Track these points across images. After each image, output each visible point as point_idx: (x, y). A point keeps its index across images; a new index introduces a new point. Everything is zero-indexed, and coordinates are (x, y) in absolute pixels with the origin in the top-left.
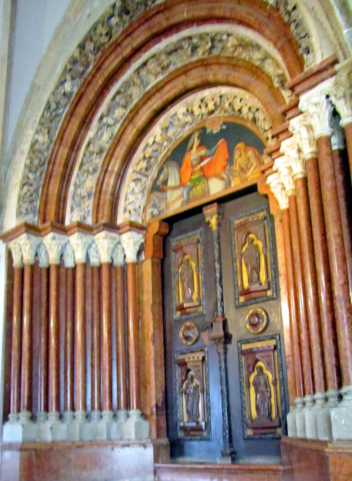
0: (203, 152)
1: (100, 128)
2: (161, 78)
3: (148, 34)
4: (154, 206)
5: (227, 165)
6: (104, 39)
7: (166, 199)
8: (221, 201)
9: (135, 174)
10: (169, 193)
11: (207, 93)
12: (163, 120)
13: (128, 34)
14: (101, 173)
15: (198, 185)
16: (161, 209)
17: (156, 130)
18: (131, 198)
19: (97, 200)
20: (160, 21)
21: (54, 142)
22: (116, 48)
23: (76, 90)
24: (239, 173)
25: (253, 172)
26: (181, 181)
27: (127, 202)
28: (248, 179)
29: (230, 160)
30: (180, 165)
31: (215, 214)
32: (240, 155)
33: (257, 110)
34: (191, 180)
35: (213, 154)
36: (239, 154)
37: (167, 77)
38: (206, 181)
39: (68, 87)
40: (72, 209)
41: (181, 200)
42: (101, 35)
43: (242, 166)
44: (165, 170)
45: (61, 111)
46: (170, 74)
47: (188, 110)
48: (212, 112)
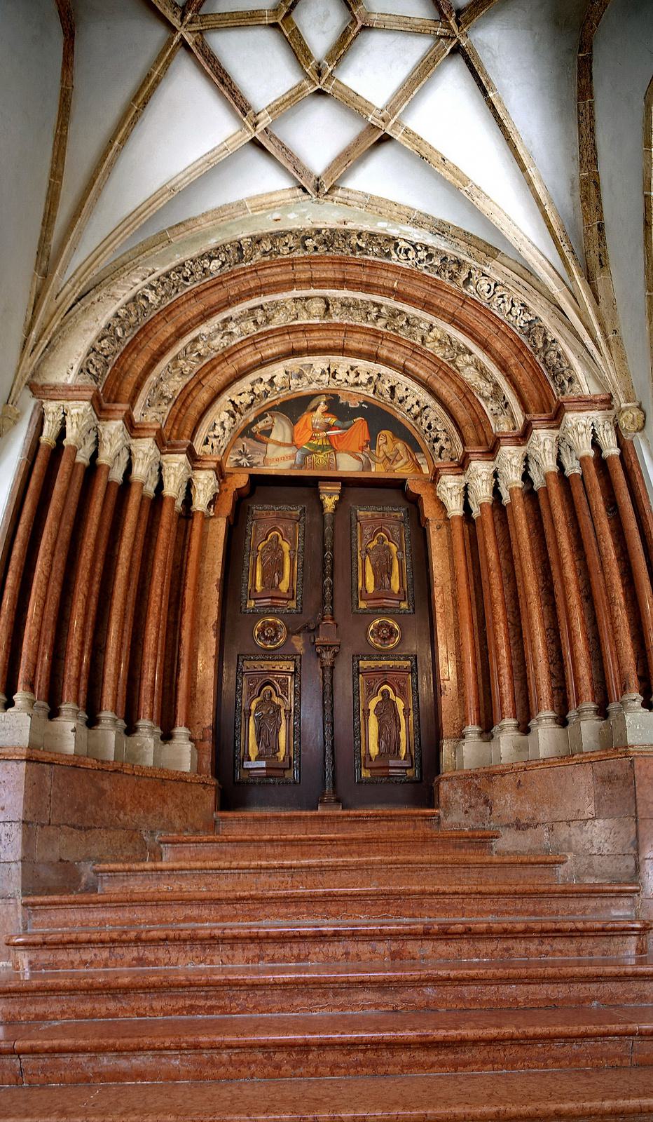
0: (333, 420)
1: (218, 330)
2: (317, 321)
8: (348, 483)
10: (270, 446)
11: (361, 363)
12: (292, 363)
13: (310, 262)
15: (319, 454)
16: (255, 461)
17: (278, 371)
20: (354, 273)
26: (293, 440)
27: (212, 434)
29: (372, 443)
30: (294, 421)
31: (336, 494)
32: (386, 443)
34: (310, 445)
35: (347, 428)
40: (145, 408)
41: (293, 461)
42: (287, 244)
43: (388, 455)
44: (269, 418)
47: (329, 369)
48: (357, 384)
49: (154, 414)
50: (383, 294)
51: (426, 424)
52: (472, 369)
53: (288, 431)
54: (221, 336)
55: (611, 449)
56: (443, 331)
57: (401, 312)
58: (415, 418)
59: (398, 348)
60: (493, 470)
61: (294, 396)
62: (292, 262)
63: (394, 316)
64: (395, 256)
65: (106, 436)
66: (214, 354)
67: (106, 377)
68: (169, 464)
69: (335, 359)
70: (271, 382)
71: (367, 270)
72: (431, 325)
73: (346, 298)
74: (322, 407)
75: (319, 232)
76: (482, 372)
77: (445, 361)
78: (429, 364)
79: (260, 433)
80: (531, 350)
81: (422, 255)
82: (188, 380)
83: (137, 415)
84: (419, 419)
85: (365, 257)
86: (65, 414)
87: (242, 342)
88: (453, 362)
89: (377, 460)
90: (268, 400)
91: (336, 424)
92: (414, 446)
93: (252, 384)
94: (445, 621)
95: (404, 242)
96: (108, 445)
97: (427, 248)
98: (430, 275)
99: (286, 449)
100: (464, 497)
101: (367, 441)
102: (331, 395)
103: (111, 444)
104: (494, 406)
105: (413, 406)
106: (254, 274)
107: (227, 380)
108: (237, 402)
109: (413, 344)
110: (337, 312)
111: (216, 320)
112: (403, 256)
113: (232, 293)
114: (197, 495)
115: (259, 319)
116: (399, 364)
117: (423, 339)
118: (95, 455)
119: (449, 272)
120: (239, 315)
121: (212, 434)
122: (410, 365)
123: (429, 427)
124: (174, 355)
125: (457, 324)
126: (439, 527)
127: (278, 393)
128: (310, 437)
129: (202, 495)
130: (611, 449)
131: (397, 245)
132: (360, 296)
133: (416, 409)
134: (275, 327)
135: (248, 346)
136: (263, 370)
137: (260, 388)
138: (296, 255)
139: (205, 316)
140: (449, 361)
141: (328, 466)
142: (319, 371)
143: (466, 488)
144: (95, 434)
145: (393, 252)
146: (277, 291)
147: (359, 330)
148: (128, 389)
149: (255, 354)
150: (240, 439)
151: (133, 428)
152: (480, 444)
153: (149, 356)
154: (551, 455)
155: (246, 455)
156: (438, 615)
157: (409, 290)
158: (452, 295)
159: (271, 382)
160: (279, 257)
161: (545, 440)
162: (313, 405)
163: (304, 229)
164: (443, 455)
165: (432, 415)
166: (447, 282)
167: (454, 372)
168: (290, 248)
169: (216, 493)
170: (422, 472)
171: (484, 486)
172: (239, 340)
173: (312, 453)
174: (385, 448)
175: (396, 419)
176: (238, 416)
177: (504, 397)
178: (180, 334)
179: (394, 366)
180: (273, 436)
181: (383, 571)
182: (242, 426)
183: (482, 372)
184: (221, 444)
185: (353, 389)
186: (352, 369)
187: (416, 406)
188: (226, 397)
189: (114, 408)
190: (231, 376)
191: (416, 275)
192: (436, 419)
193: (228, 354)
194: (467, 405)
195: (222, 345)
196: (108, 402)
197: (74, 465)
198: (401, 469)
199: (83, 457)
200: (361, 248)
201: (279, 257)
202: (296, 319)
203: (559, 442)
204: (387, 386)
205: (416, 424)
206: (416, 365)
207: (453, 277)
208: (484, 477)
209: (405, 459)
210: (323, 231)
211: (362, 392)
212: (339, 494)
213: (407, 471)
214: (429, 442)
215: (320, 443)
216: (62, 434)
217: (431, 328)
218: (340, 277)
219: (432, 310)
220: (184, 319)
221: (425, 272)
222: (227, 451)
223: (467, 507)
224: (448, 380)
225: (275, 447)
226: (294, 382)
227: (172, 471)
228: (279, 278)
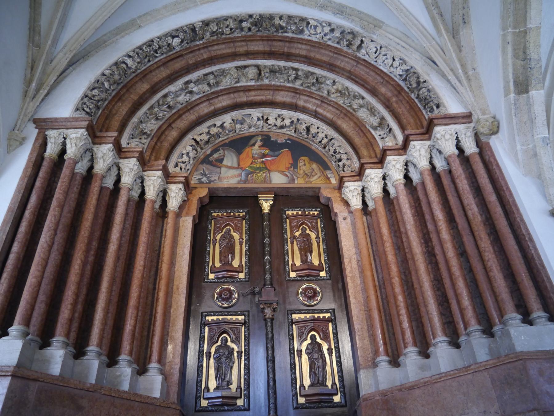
0: (267, 151)
1: (182, 90)
2: (252, 83)
3: (267, 49)
4: (204, 175)
5: (291, 167)
6: (227, 31)
10: (223, 170)
12: (236, 114)
13: (246, 40)
14: (163, 124)
15: (258, 173)
16: (212, 179)
17: (227, 119)
18: (185, 158)
19: (153, 143)
20: (278, 46)
21: (136, 73)
22: (230, 42)
23: (178, 49)
24: (303, 177)
25: (317, 179)
26: (239, 164)
28: (312, 183)
29: (295, 165)
34: (250, 167)
35: (277, 156)
36: (303, 163)
37: (258, 86)
38: (267, 172)
39: (176, 41)
40: (129, 139)
41: (239, 179)
43: (306, 172)
44: (221, 151)
45: (157, 55)
46: (261, 85)
47: (263, 117)
48: (282, 127)
49: (137, 143)
50: (299, 62)
51: (332, 150)
52: (364, 110)
53: (235, 159)
54: (184, 94)
55: (470, 148)
56: (343, 85)
57: (313, 73)
58: (324, 148)
60: (382, 174)
61: (239, 137)
62: (233, 41)
63: (307, 77)
64: (307, 32)
65: (100, 155)
66: (180, 106)
67: (98, 116)
68: (149, 178)
70: (222, 126)
71: (287, 44)
72: (334, 81)
73: (273, 65)
75: (251, 16)
76: (372, 111)
77: (345, 106)
78: (334, 110)
79: (215, 161)
80: (407, 90)
81: (327, 29)
82: (161, 123)
83: (124, 142)
84: (327, 148)
85: (286, 34)
86: (65, 138)
87: (200, 98)
88: (350, 106)
89: (298, 175)
90: (220, 139)
91: (268, 154)
92: (325, 166)
93: (209, 127)
94: (354, 282)
95: (313, 21)
96: (101, 161)
97: (330, 25)
98: (333, 45)
99: (234, 170)
100: (362, 197)
101: (291, 164)
102: (265, 135)
103: (104, 160)
105: (323, 139)
106: (206, 50)
108: (198, 140)
109: (322, 96)
110: (267, 75)
111: (180, 83)
112: (312, 32)
113: (191, 62)
114: (171, 200)
115: (212, 82)
116: (312, 111)
117: (328, 92)
118: (91, 168)
119: (346, 41)
120: (196, 78)
121: (180, 160)
122: (320, 110)
123: (335, 152)
124: (150, 106)
125: (352, 79)
126: (345, 219)
127: (227, 135)
128: (250, 162)
129: (174, 200)
130: (470, 148)
131: (308, 23)
132: (282, 63)
133: (325, 141)
134: (224, 88)
135: (205, 101)
136: (216, 119)
137: (214, 130)
138: (236, 35)
139: (171, 79)
140: (348, 106)
141: (264, 181)
142: (256, 118)
143: (363, 190)
144: (91, 154)
145: (305, 29)
146: (223, 62)
147: (283, 88)
148: (116, 123)
149: (210, 106)
150: (201, 165)
151: (120, 151)
152: (371, 157)
153: (131, 104)
154: (425, 158)
155: (206, 175)
156: (348, 278)
157: (318, 56)
158: (349, 58)
159: (222, 126)
160: (224, 36)
161: (421, 148)
162: (252, 142)
163: (241, 15)
165: (336, 144)
166: (345, 49)
167: (351, 113)
168: (231, 29)
169: (185, 201)
170: (330, 183)
171: (376, 186)
172: (198, 97)
173: (253, 173)
174: (304, 167)
175: (311, 149)
176: (199, 149)
178: (153, 91)
179: (308, 113)
180: (225, 162)
181: (306, 249)
182: (202, 157)
183: (372, 111)
184: (188, 167)
185: (280, 131)
186: (279, 116)
187: (325, 139)
188: (190, 136)
189: (105, 135)
191: (323, 46)
192: (340, 146)
193: (190, 107)
194: (362, 134)
195: (185, 100)
196: (101, 131)
197: (73, 174)
198: (316, 181)
199: (81, 168)
200: (282, 28)
201: (224, 36)
202: (237, 82)
203: (431, 149)
204: (304, 126)
205: (326, 152)
206: (324, 110)
207: (349, 45)
208: (376, 179)
209: (319, 175)
210: (254, 16)
212: (273, 200)
213: (320, 182)
214: (335, 162)
215: (258, 166)
216: (63, 151)
217: (334, 82)
218: (268, 49)
219: (334, 71)
220: (156, 80)
221: (329, 43)
222: (192, 173)
223: (364, 203)
224: (347, 119)
225: (226, 169)
226: (238, 126)
227: (151, 182)
228: (224, 51)
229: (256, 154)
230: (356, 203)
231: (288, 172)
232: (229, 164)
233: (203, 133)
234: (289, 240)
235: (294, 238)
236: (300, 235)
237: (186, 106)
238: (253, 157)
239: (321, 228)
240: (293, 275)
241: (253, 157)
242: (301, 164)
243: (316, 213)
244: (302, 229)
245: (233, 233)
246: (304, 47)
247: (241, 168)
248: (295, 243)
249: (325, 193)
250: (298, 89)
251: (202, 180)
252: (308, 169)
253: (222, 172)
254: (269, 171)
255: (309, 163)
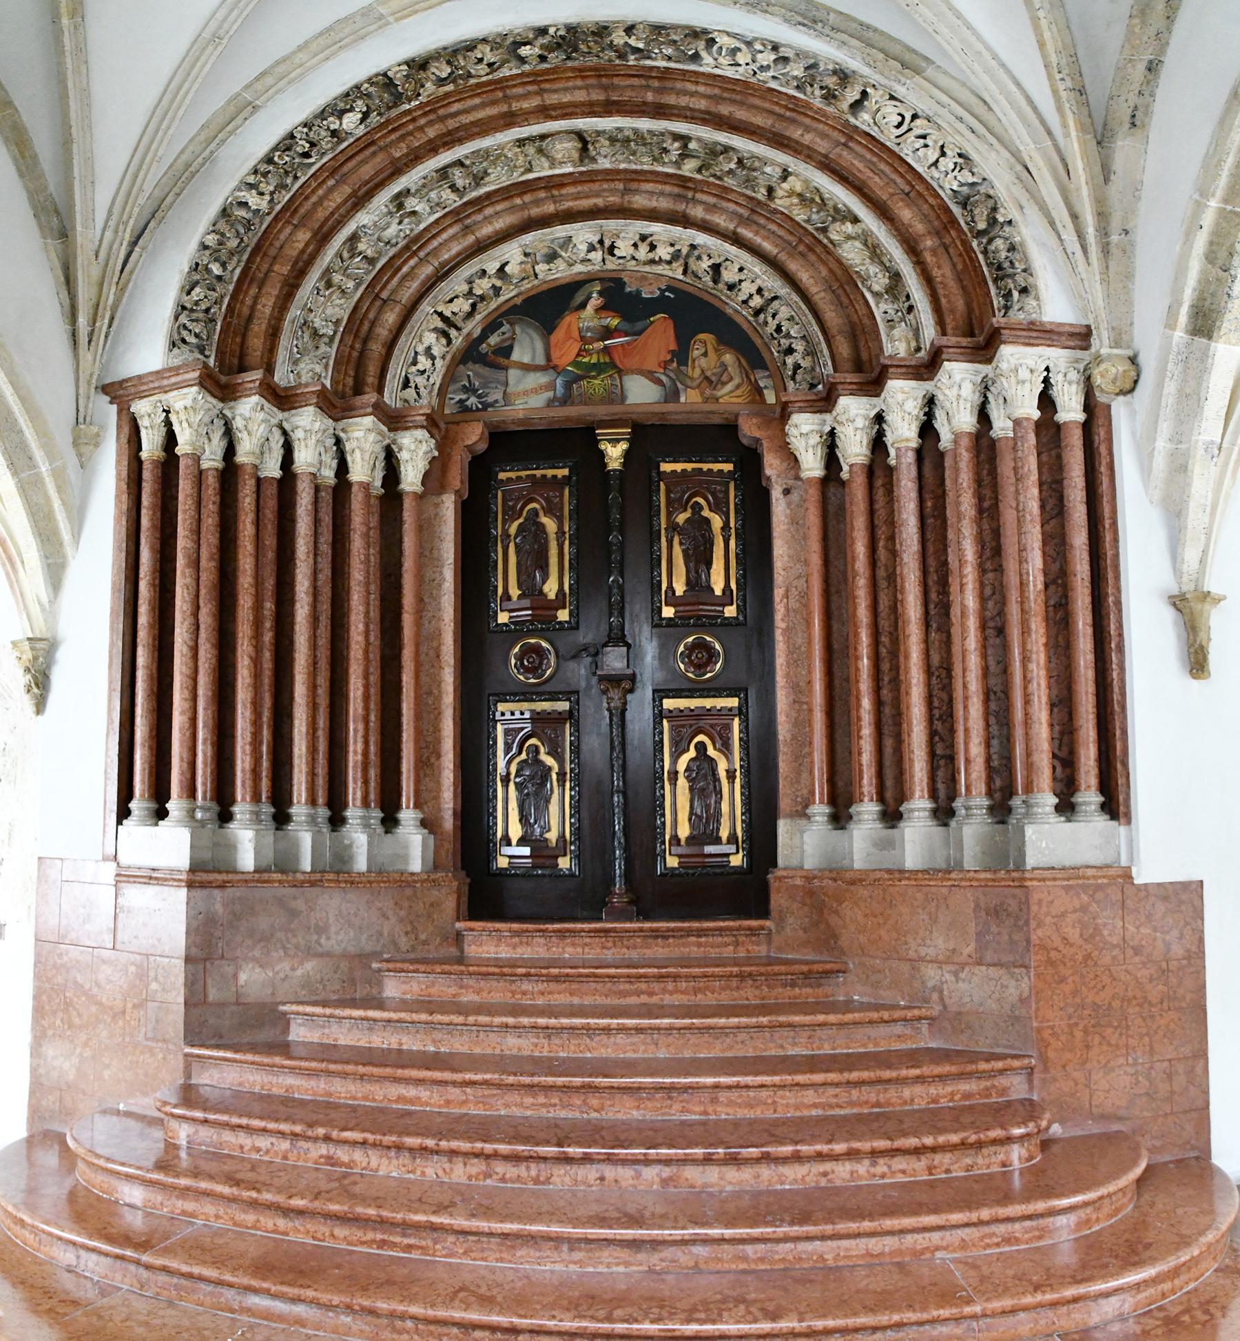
5: (672, 361)
7: (507, 384)
9: (435, 316)
10: (513, 374)
15: (594, 378)
25: (732, 392)
29: (681, 355)
33: (775, 298)
34: (575, 363)
43: (708, 374)
52: (857, 244)
53: (539, 345)
57: (727, 149)
59: (725, 204)
69: (612, 224)
72: (785, 170)
74: (595, 301)
76: (875, 252)
77: (809, 228)
79: (494, 352)
89: (689, 382)
91: (620, 327)
99: (538, 374)
101: (672, 352)
104: (890, 307)
105: (751, 296)
107: (423, 283)
108: (448, 313)
123: (779, 329)
128: (576, 351)
133: (757, 301)
135: (450, 225)
137: (482, 287)
140: (817, 229)
164: (798, 378)
165: (784, 312)
173: (581, 378)
174: (703, 362)
177: (908, 297)
180: (516, 356)
188: (426, 307)
190: (429, 278)
192: (791, 319)
206: (757, 233)
209: (737, 381)
211: (665, 272)
213: (739, 400)
221: (773, 85)
229: (588, 329)
230: (812, 465)
231: (664, 374)
232: (526, 360)
233: (457, 297)
234: (663, 532)
235: (673, 527)
236: (687, 520)
237: (407, 247)
238: (582, 338)
239: (736, 505)
240: (668, 612)
241: (582, 338)
242: (696, 353)
243: (728, 467)
244: (692, 507)
245: (545, 520)
246: (701, 89)
247: (555, 368)
248: (676, 540)
249: (749, 429)
250: (690, 179)
251: (468, 403)
252: (713, 365)
253: (511, 380)
254: (621, 373)
255: (716, 350)
